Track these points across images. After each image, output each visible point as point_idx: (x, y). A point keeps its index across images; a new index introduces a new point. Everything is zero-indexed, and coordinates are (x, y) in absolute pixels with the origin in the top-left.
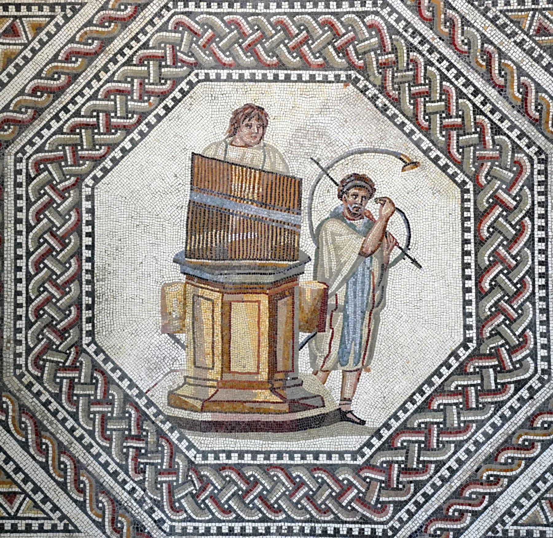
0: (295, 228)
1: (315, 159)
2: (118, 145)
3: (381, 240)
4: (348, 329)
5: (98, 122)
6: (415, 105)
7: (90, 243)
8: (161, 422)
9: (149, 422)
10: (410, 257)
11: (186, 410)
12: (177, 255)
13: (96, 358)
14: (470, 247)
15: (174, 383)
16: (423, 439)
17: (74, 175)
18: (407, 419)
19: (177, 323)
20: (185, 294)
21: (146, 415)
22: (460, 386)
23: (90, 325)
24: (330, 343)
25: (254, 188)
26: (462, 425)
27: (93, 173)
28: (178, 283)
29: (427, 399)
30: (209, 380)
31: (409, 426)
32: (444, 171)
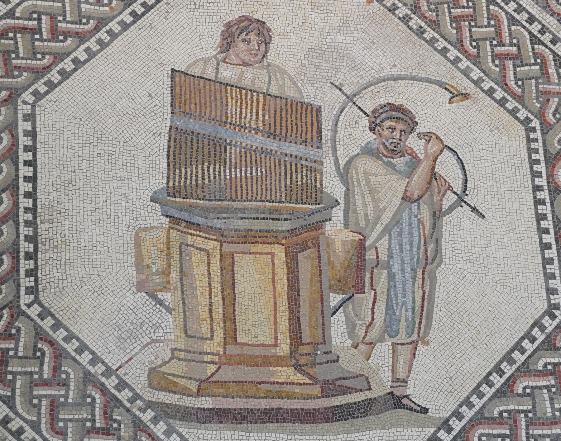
0: (316, 165)
1: (337, 84)
2: (68, 55)
3: (429, 183)
4: (395, 290)
5: (40, 27)
6: (459, 29)
7: (31, 174)
8: (139, 409)
9: (121, 409)
10: (468, 205)
11: (175, 393)
12: (155, 192)
13: (41, 323)
14: (544, 195)
15: (157, 357)
16: (508, 432)
17: (7, 89)
18: (484, 406)
19: (158, 279)
20: (168, 243)
21: (117, 400)
22: (549, 364)
23: (32, 279)
24: (373, 308)
25: (257, 114)
26: (558, 414)
27: (33, 88)
28: (157, 227)
29: (508, 380)
30: (207, 354)
31: (486, 415)
32: (501, 106)
